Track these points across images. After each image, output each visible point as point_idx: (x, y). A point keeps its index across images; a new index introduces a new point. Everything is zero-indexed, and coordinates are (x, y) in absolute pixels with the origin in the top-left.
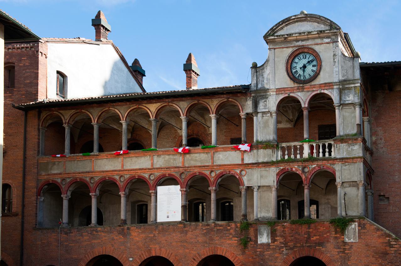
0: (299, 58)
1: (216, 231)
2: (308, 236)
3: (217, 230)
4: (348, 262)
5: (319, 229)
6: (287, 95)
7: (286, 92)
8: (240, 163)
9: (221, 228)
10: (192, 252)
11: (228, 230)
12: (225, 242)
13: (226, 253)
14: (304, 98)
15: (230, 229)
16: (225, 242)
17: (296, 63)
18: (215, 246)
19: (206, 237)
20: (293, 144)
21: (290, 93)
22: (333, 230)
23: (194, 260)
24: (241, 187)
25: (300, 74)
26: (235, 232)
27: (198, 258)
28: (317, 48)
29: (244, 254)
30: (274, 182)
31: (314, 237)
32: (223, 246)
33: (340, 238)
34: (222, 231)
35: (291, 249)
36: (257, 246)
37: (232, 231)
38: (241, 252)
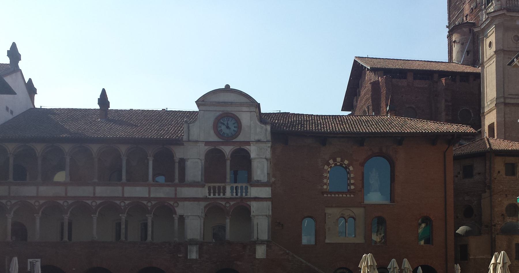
6: (213, 147)
8: (173, 196)
14: (227, 150)
20: (217, 185)
24: (174, 216)
25: (224, 132)
28: (237, 114)
30: (202, 213)
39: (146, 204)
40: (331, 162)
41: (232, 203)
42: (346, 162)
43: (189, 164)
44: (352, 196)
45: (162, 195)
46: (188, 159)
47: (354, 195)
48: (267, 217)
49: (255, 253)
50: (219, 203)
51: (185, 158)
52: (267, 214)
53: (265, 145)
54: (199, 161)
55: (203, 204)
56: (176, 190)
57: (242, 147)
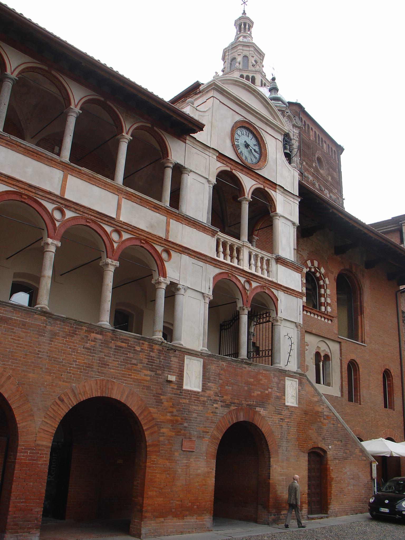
0: (242, 131)
1: (115, 349)
3: (116, 346)
4: (287, 435)
5: (261, 380)
6: (228, 169)
7: (228, 164)
9: (123, 345)
10: (60, 382)
11: (136, 352)
12: (129, 375)
13: (127, 397)
15: (141, 352)
16: (129, 375)
17: (238, 134)
18: (109, 379)
19: (93, 356)
21: (234, 169)
23: (62, 401)
26: (148, 359)
27: (70, 398)
29: (158, 405)
30: (209, 288)
31: (255, 392)
32: (123, 382)
34: (126, 351)
35: (228, 406)
36: (181, 392)
37: (142, 356)
38: (155, 399)
39: (109, 232)
40: (309, 263)
41: (254, 285)
42: (323, 270)
44: (330, 322)
45: (142, 226)
46: (191, 171)
47: (331, 321)
48: (297, 327)
50: (236, 276)
51: (186, 167)
53: (293, 200)
54: (207, 185)
55: (214, 271)
56: (168, 224)
57: (266, 189)
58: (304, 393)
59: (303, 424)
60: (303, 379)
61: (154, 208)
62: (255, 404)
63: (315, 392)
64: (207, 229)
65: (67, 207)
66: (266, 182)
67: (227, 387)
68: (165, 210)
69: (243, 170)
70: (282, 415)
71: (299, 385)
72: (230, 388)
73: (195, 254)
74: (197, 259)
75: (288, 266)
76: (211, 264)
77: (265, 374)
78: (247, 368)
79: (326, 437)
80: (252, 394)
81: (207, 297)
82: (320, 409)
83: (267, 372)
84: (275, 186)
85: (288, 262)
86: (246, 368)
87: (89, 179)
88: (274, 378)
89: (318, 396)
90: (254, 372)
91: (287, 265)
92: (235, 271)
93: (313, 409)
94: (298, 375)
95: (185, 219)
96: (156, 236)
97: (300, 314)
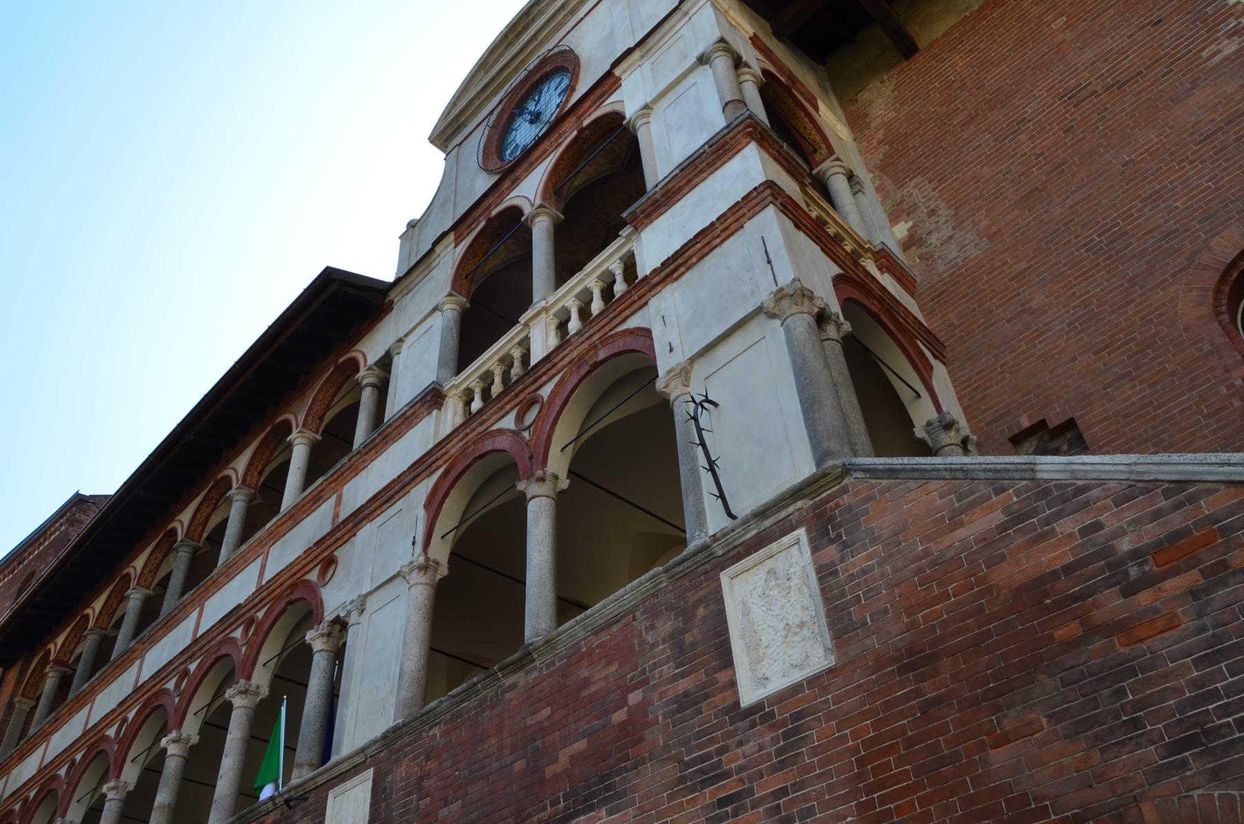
2: (528, 765)
5: (587, 682)
22: (663, 651)
30: (414, 544)
33: (706, 697)
43: (399, 363)
46: (401, 340)
48: (772, 316)
49: (725, 657)
52: (764, 293)
58: (869, 557)
59: (909, 743)
60: (845, 490)
61: (314, 504)
62: (567, 808)
63: (966, 486)
64: (412, 415)
65: (191, 659)
66: (580, 113)
67: (444, 812)
68: (329, 484)
69: (517, 179)
70: (727, 775)
71: (814, 550)
72: (456, 806)
73: (377, 504)
74: (388, 505)
75: (681, 189)
76: (419, 479)
77: (602, 645)
78: (521, 683)
79: (1225, 711)
80: (549, 772)
81: (411, 571)
82: (1052, 556)
83: (615, 628)
84: (611, 81)
85: (669, 186)
86: (514, 686)
87: (227, 577)
88: (652, 627)
89: (999, 491)
90: (550, 675)
91: (676, 193)
92: (481, 424)
93: (979, 596)
94: (799, 504)
95: (366, 453)
96: (299, 557)
97: (769, 262)
